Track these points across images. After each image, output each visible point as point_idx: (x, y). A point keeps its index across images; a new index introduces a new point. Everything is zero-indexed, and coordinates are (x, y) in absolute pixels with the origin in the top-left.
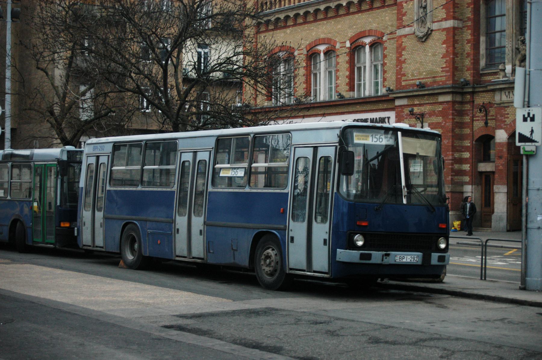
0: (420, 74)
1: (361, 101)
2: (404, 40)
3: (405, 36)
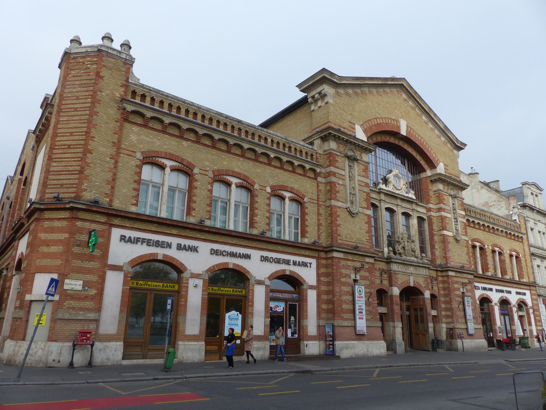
0: (352, 239)
1: (290, 244)
3: (339, 207)
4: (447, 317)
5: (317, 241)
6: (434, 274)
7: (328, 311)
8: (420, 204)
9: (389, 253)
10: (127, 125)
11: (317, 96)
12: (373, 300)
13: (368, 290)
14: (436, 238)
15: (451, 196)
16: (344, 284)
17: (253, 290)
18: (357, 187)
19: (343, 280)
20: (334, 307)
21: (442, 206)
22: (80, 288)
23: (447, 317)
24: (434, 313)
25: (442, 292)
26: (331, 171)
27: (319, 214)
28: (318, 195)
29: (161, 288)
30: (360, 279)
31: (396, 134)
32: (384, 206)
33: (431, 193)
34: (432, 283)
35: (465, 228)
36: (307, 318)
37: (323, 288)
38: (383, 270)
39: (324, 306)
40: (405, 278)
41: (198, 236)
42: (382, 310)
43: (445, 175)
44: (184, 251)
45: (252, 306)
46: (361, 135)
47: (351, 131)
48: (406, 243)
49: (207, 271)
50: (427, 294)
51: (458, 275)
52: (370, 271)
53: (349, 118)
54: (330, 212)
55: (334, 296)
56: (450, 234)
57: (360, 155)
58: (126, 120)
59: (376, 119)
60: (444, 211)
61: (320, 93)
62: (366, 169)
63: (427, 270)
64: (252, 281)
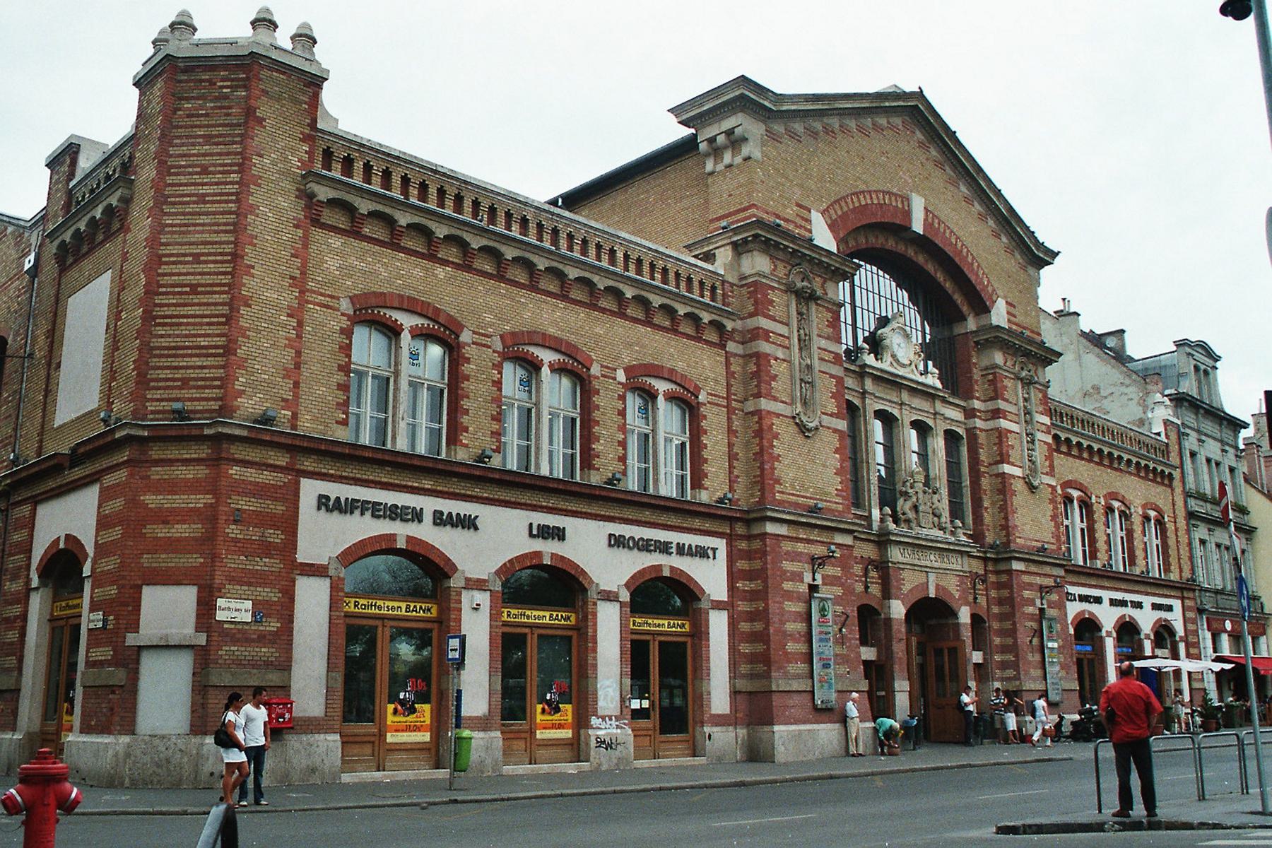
2: (775, 421)
3: (778, 415)
4: (1004, 665)
5: (730, 496)
6: (978, 567)
7: (753, 659)
8: (951, 400)
9: (882, 520)
10: (317, 234)
11: (721, 139)
12: (851, 632)
13: (839, 609)
14: (985, 482)
15: (1022, 380)
16: (789, 595)
17: (595, 615)
18: (817, 365)
19: (787, 586)
20: (768, 648)
21: (1002, 405)
22: (248, 618)
23: (1004, 665)
24: (977, 657)
25: (995, 610)
26: (758, 328)
27: (731, 431)
28: (729, 386)
29: (403, 613)
30: (824, 584)
31: (901, 230)
32: (873, 405)
33: (977, 374)
34: (974, 588)
35: (1049, 458)
36: (709, 675)
37: (743, 606)
38: (871, 562)
39: (745, 648)
40: (919, 578)
41: (477, 492)
42: (868, 653)
43: (1009, 331)
44: (448, 527)
45: (595, 650)
46: (824, 238)
47: (801, 227)
48: (921, 495)
49: (498, 573)
50: (964, 616)
51: (1033, 568)
52: (844, 564)
53: (797, 194)
54: (756, 427)
55: (767, 624)
56: (1018, 472)
57: (822, 286)
58: (316, 222)
59: (856, 194)
60: (1005, 418)
61: (730, 133)
62: (835, 322)
63: (966, 558)
64: (592, 594)
